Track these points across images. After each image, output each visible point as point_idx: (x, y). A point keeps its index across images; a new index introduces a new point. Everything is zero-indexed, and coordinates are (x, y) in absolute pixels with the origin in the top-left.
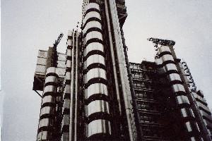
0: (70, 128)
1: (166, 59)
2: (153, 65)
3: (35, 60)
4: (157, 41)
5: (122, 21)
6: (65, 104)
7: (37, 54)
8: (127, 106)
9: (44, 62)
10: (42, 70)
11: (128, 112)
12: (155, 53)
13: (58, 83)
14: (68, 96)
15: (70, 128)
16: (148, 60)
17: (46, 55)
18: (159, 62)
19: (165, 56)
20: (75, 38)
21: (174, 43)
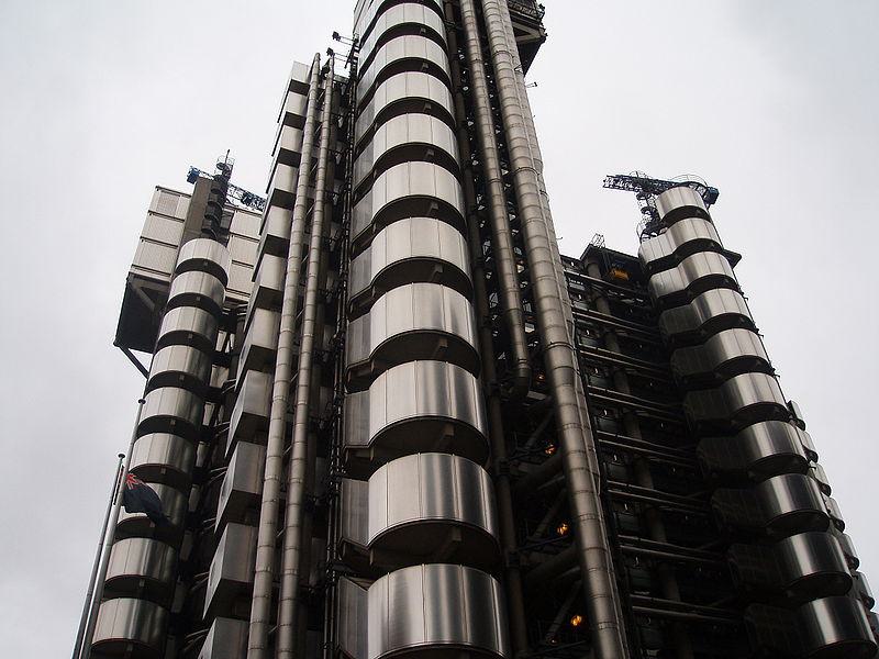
0: (275, 429)
1: (690, 236)
2: (639, 270)
3: (138, 222)
4: (646, 187)
5: (528, 52)
6: (259, 330)
7: (147, 199)
8: (553, 336)
9: (173, 232)
10: (161, 262)
11: (559, 358)
12: (639, 220)
13: (225, 315)
14: (263, 360)
15: (275, 429)
16: (613, 244)
17: (182, 208)
18: (662, 246)
19: (687, 222)
20: (320, 91)
21: (711, 196)
